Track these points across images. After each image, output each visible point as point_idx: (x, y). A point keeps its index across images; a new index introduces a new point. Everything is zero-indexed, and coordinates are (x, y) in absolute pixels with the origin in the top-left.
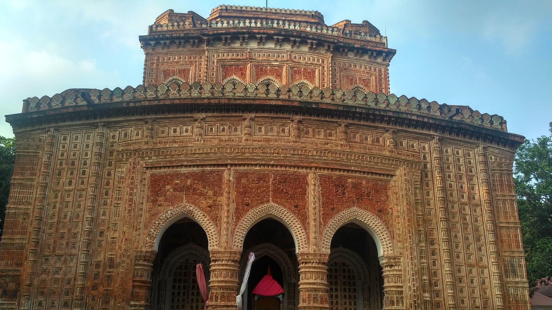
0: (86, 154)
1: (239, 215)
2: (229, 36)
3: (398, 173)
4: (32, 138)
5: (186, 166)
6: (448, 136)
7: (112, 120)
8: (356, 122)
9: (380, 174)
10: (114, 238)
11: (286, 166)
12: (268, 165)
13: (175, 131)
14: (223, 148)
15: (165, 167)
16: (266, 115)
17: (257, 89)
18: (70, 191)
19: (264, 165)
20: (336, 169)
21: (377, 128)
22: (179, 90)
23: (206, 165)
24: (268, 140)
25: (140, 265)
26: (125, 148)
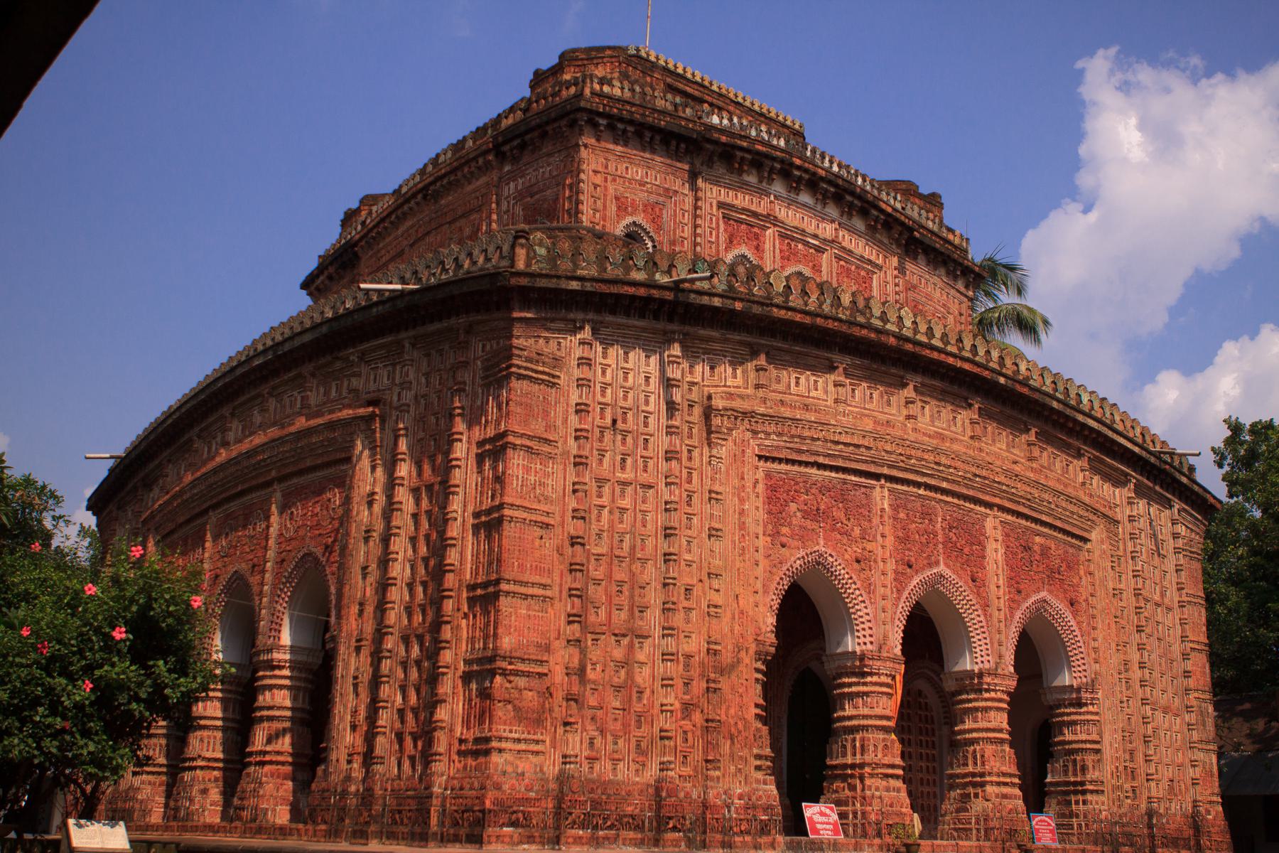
0: (647, 403)
2: (748, 156)
3: (1094, 536)
4: (545, 338)
5: (821, 466)
6: (1145, 481)
7: (702, 332)
10: (716, 607)
13: (797, 384)
15: (788, 461)
16: (937, 383)
18: (625, 484)
21: (1069, 446)
25: (757, 670)
26: (728, 404)
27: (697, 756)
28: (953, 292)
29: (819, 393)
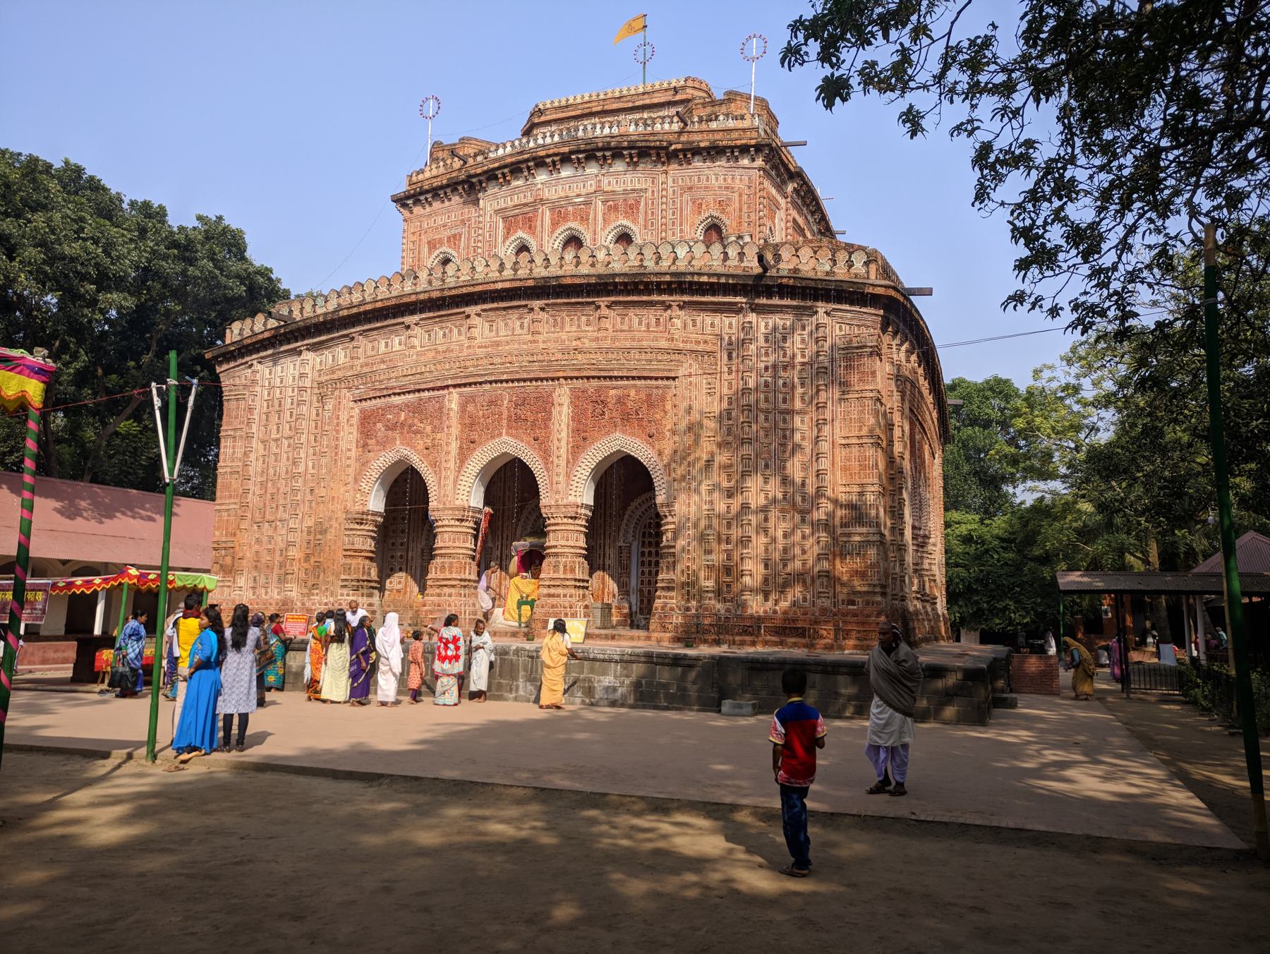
1: (463, 457)
5: (399, 394)
8: (621, 299)
9: (656, 379)
11: (525, 380)
12: (501, 382)
14: (440, 362)
16: (495, 305)
17: (487, 265)
19: (496, 382)
20: (593, 377)
22: (390, 285)
23: (423, 390)
24: (497, 344)
27: (310, 584)
28: (738, 172)
29: (403, 347)
